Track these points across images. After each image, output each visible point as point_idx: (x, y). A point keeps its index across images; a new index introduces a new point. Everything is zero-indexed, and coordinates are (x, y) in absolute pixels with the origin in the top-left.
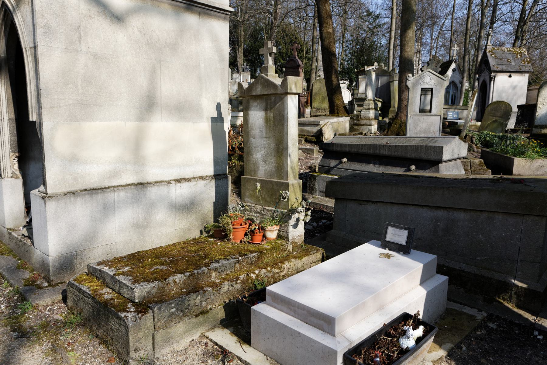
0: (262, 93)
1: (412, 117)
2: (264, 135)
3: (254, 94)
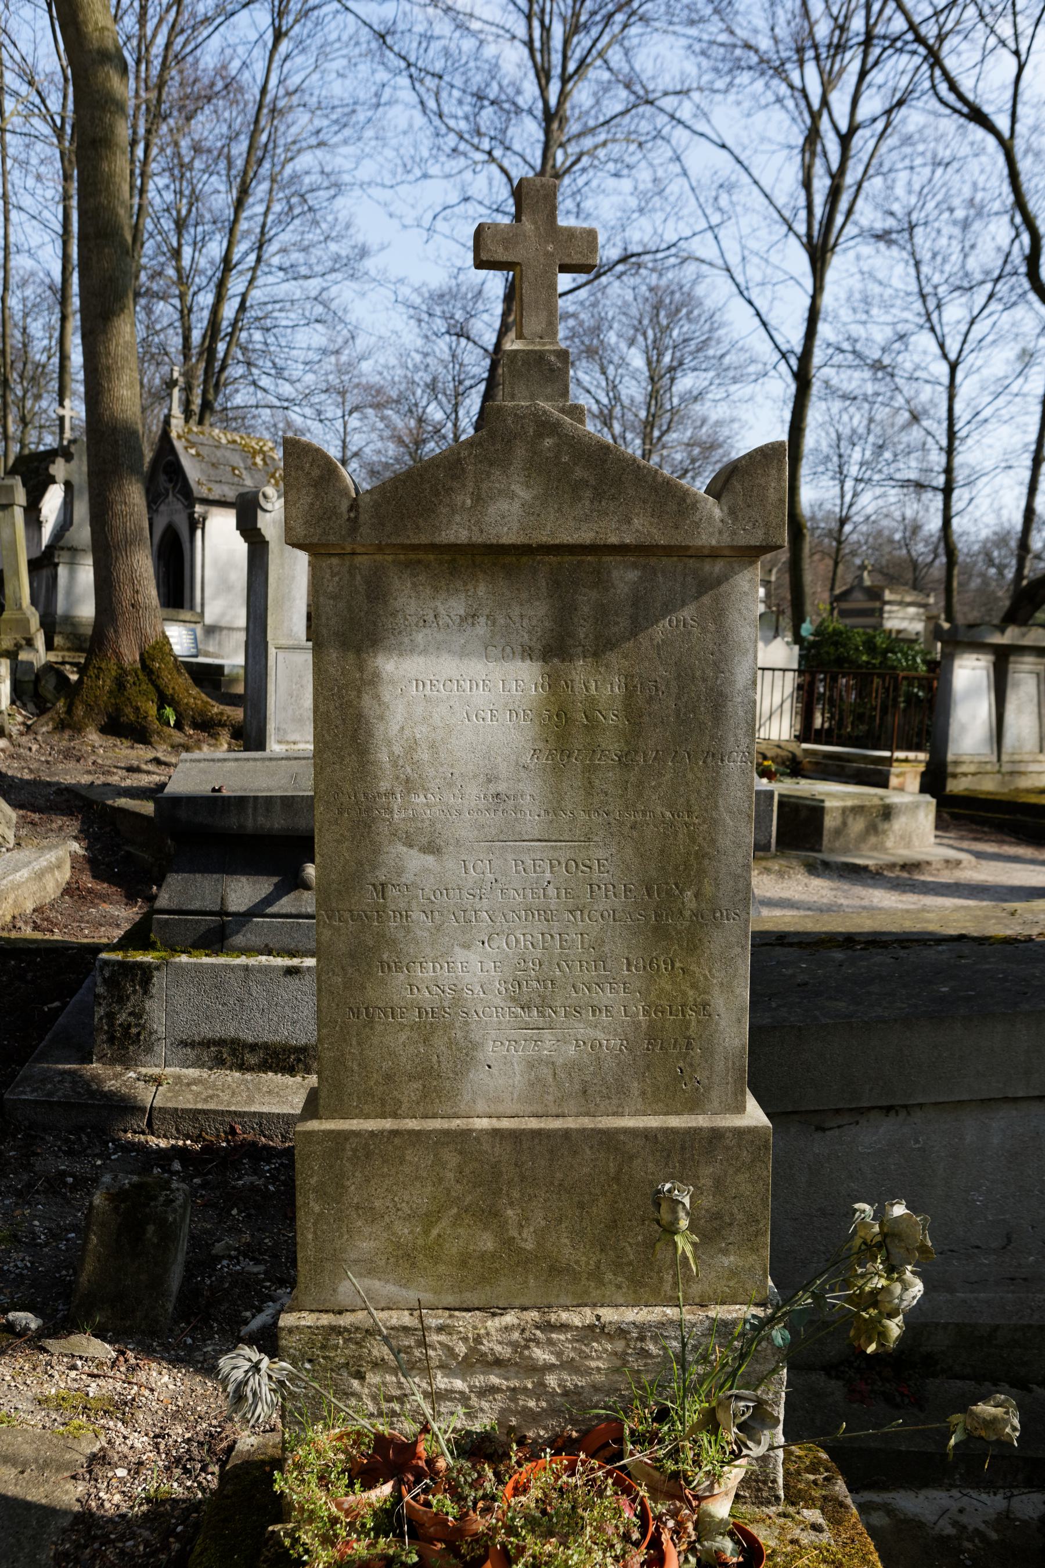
0: (543, 537)
1: (281, 655)
2: (532, 821)
3: (457, 532)
